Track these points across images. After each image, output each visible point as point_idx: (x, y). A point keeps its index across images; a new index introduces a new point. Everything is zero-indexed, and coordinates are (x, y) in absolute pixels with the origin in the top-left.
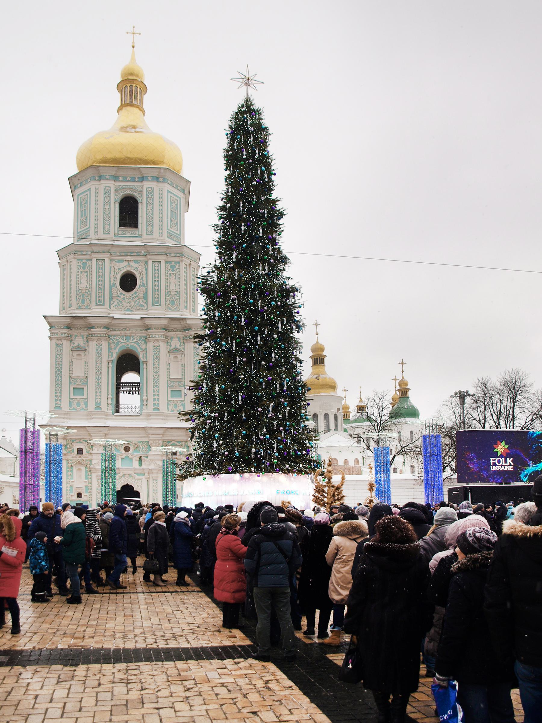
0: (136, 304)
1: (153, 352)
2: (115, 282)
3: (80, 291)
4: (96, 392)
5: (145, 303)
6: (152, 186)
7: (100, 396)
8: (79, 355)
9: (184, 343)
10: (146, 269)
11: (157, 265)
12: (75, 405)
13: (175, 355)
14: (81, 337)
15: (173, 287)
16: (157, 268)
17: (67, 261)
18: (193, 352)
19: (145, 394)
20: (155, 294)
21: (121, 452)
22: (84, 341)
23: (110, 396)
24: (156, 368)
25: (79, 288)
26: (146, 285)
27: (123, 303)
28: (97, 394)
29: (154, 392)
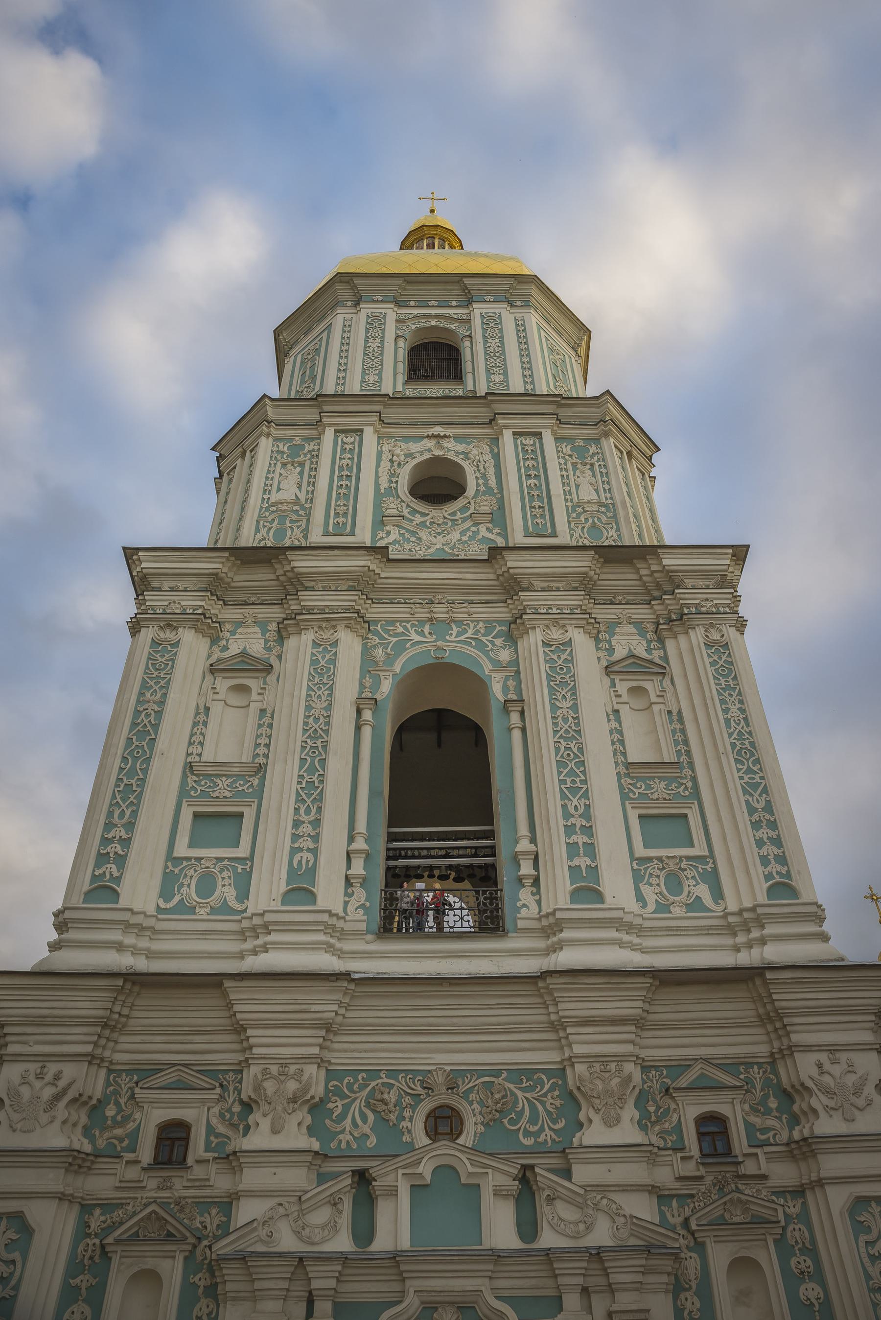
0: (465, 538)
1: (546, 661)
2: (394, 485)
3: (272, 509)
4: (297, 824)
5: (498, 534)
6: (497, 311)
7: (316, 838)
8: (243, 689)
9: (661, 641)
10: (497, 457)
11: (529, 441)
12: (189, 892)
13: (634, 684)
14: (257, 629)
15: (587, 493)
16: (529, 448)
17: (243, 455)
19: (523, 829)
20: (534, 507)
21: (412, 1143)
22: (267, 641)
23: (360, 844)
24: (565, 720)
26: (496, 491)
27: (423, 534)
28: (300, 831)
29: (567, 815)
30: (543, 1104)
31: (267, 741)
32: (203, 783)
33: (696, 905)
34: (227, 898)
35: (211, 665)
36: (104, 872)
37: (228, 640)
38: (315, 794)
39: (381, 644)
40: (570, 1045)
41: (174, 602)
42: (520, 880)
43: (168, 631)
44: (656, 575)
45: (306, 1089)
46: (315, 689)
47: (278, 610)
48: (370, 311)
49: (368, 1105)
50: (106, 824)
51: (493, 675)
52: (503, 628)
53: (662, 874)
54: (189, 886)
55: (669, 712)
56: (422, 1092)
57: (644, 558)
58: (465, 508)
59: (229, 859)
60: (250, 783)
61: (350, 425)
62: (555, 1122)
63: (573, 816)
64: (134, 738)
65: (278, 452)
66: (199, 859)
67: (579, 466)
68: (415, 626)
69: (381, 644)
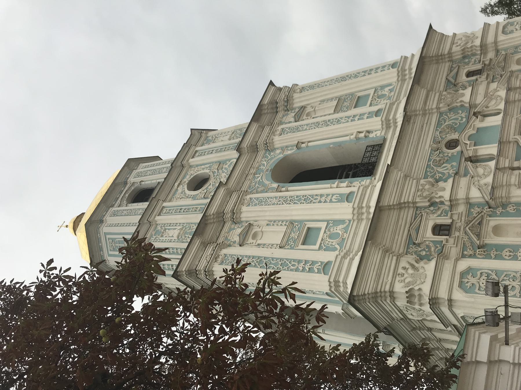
0: (226, 171)
4: (320, 202)
5: (229, 162)
6: (136, 173)
7: (328, 195)
8: (255, 236)
10: (197, 166)
12: (335, 242)
13: (305, 115)
14: (231, 232)
16: (200, 154)
18: (306, 92)
22: (239, 227)
25: (176, 238)
26: (212, 164)
28: (323, 201)
30: (450, 118)
31: (281, 222)
32: (290, 243)
33: (391, 91)
34: (342, 227)
35: (240, 246)
36: (317, 269)
37: (231, 242)
38: (310, 197)
39: (257, 189)
40: (432, 109)
41: (206, 257)
42: (365, 136)
43: (218, 259)
44: (269, 108)
45: (429, 182)
46: (266, 203)
47: (227, 224)
48: (109, 216)
49: (440, 166)
50: (295, 271)
51: (284, 153)
52: (268, 153)
53: (377, 99)
54: (332, 242)
55: (320, 104)
56: (439, 151)
57: (262, 110)
58: (214, 173)
59: (326, 228)
60: (296, 226)
61: (158, 211)
62: (459, 113)
63: (348, 120)
64: (261, 265)
65: (154, 240)
66: (322, 240)
67: (214, 141)
68: (254, 179)
69: (257, 189)
